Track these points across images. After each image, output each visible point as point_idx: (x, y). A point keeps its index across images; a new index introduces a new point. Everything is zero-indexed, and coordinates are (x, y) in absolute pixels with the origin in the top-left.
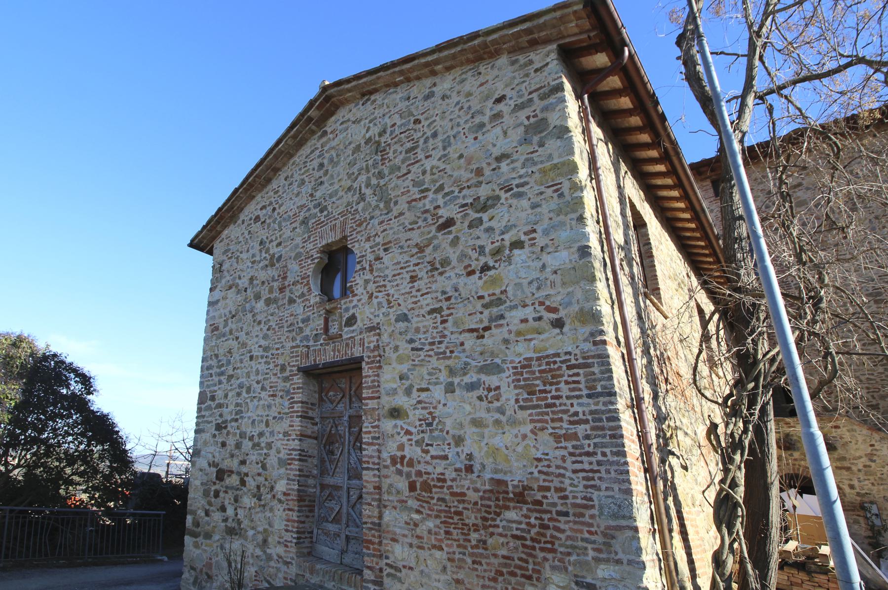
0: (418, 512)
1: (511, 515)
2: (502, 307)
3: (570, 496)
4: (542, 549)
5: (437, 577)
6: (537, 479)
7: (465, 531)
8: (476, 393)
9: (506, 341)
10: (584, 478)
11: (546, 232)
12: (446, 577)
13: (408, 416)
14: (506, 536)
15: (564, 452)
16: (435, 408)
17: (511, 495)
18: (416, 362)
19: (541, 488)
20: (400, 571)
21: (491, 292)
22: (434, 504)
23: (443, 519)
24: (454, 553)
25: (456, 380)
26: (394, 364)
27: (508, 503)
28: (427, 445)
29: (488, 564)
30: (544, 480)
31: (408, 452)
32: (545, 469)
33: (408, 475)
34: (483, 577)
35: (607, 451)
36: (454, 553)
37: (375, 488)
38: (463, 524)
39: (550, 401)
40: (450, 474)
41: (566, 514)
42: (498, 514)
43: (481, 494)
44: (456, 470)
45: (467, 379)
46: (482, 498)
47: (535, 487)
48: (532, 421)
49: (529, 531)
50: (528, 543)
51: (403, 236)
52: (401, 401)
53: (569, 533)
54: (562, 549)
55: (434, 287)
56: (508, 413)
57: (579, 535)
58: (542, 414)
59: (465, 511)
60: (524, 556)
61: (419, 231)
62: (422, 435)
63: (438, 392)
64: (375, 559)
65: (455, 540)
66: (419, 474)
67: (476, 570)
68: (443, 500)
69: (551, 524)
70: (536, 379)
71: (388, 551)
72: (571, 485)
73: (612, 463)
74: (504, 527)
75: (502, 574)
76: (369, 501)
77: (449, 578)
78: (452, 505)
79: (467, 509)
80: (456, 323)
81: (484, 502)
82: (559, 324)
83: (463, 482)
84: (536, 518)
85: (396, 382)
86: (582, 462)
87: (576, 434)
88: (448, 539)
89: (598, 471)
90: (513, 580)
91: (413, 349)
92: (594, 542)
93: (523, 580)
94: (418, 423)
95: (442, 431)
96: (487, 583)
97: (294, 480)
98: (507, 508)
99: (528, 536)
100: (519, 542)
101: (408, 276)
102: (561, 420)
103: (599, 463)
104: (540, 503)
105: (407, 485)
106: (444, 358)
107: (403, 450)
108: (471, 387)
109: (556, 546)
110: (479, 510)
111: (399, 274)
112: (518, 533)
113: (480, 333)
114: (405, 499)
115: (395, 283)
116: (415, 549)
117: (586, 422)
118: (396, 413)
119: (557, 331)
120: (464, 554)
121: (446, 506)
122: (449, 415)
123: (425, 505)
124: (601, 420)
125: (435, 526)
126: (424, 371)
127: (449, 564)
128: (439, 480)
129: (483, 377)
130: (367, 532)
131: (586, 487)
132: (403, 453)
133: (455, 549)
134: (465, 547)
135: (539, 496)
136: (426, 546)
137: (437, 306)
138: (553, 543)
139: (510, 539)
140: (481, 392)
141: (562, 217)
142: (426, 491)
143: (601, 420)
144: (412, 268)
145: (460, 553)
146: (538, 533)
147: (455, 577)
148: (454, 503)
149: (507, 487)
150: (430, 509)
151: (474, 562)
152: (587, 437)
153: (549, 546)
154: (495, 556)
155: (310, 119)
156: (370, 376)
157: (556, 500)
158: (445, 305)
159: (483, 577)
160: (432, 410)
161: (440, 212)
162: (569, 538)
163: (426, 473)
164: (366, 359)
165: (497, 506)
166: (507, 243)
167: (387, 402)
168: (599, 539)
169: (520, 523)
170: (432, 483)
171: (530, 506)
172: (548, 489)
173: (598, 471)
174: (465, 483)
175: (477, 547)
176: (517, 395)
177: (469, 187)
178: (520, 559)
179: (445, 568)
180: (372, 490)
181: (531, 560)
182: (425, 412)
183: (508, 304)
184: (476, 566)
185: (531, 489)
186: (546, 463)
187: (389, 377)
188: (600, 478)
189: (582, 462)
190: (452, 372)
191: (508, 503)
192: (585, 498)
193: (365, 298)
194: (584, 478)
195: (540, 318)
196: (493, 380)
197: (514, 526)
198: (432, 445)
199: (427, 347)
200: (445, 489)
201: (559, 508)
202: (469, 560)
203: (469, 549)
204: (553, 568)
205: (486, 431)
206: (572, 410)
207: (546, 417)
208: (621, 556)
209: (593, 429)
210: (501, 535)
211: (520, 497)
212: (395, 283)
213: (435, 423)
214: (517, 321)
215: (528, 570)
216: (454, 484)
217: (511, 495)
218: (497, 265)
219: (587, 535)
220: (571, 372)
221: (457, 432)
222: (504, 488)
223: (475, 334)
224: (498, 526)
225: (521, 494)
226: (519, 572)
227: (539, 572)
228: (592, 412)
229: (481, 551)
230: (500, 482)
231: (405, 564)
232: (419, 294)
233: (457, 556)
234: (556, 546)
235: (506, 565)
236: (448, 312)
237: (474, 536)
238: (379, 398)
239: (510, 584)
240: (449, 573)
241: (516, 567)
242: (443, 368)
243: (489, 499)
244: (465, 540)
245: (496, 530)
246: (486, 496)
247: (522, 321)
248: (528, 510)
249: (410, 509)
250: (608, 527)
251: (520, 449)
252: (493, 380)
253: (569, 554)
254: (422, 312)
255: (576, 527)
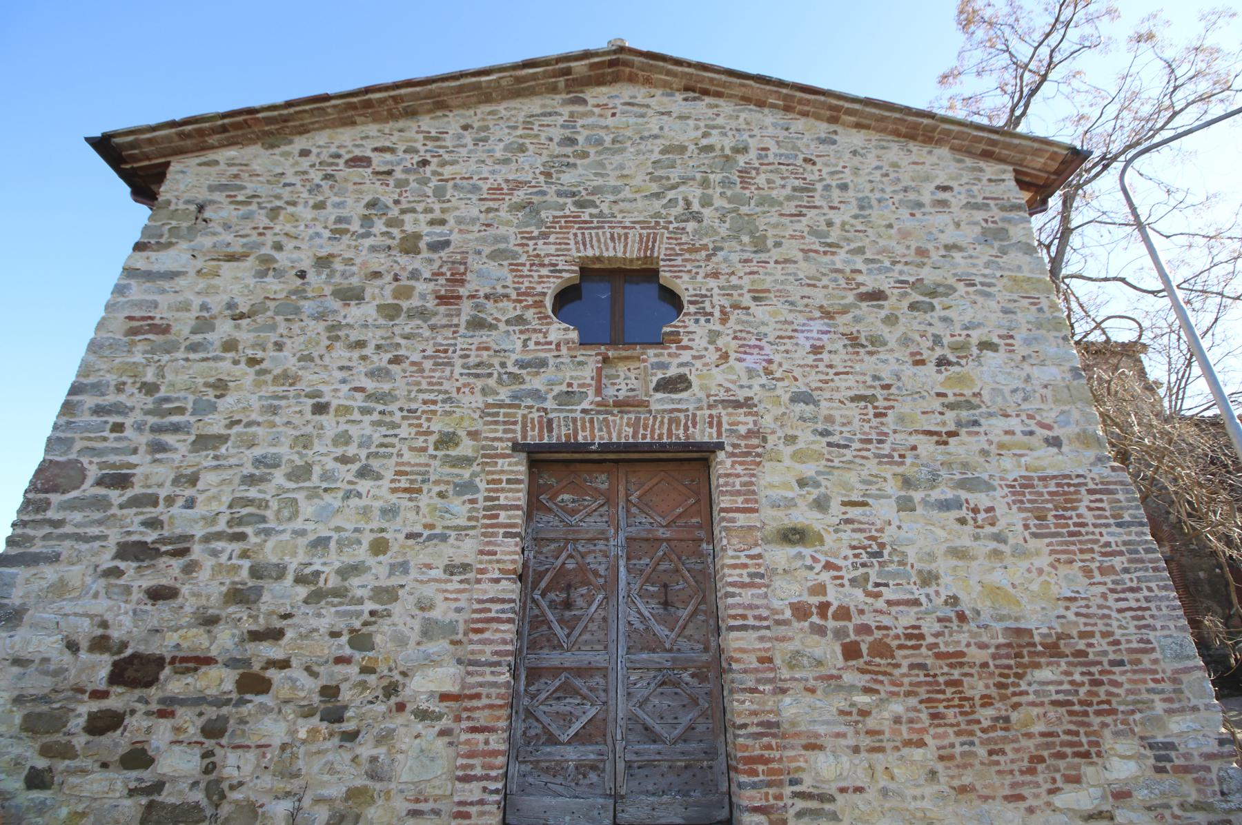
0: (867, 690)
1: (1045, 674)
2: (977, 412)
3: (1123, 640)
4: (1098, 713)
5: (918, 792)
6: (1076, 624)
7: (967, 709)
8: (956, 514)
9: (984, 453)
10: (1134, 618)
11: (1027, 342)
12: (936, 788)
13: (821, 541)
14: (1042, 704)
15: (1102, 589)
16: (881, 530)
17: (1040, 648)
18: (836, 463)
19: (1083, 635)
20: (832, 799)
21: (957, 391)
22: (904, 675)
23: (925, 696)
24: (952, 746)
25: (917, 496)
26: (787, 462)
27: (1037, 659)
28: (877, 585)
29: (1017, 750)
30: (1086, 624)
31: (833, 597)
32: (1084, 611)
33: (839, 633)
34: (1011, 772)
35: (1153, 585)
36: (952, 746)
37: (761, 660)
38: (961, 699)
39: (1072, 528)
40: (929, 626)
41: (1121, 663)
42: (1019, 676)
43: (992, 650)
44: (940, 620)
45: (936, 494)
46: (994, 657)
47: (1074, 633)
48: (1052, 552)
49: (1077, 692)
50: (1077, 708)
51: (796, 292)
52: (803, 516)
53: (1126, 686)
54: (1121, 708)
55: (858, 367)
56: (1011, 541)
57: (1142, 687)
58: (1067, 543)
59: (965, 679)
60: (1073, 727)
61: (825, 291)
62: (862, 570)
63: (884, 510)
64: (771, 791)
65: (952, 725)
66: (864, 629)
67: (997, 763)
68: (922, 666)
69: (1104, 678)
70: (1047, 501)
71: (799, 769)
72: (1120, 627)
73: (1161, 599)
74: (1036, 692)
75: (1041, 760)
76: (751, 684)
77: (945, 788)
78: (938, 672)
79: (971, 675)
80: (901, 419)
81: (998, 662)
82: (1055, 442)
83: (956, 637)
84: (1083, 674)
85: (792, 489)
86: (1126, 599)
87: (1113, 567)
88: (939, 725)
89: (1148, 609)
90: (1062, 764)
91: (829, 444)
92: (1162, 691)
93: (1077, 760)
94: (850, 553)
95: (902, 563)
96: (1019, 778)
97: (498, 664)
98: (1037, 666)
99: (1075, 699)
100: (1063, 710)
101: (808, 344)
102: (1092, 551)
103: (1147, 599)
104: (1082, 653)
105: (838, 649)
106: (891, 463)
107: (825, 594)
108: (945, 505)
109: (1114, 705)
110: (992, 674)
111: (791, 338)
112: (1061, 697)
113: (942, 438)
114: (835, 672)
115: (782, 348)
116: (864, 754)
117: (1121, 553)
118: (794, 536)
119: (1055, 450)
120: (972, 744)
121: (927, 675)
122: (911, 542)
123: (881, 678)
124: (1137, 552)
125: (908, 710)
126: (852, 477)
127: (940, 767)
128: (909, 637)
129: (964, 495)
130: (749, 742)
131: (1139, 628)
132: (823, 599)
133: (952, 738)
134: (972, 733)
135: (1081, 645)
136: (889, 745)
137: (869, 392)
138: (1108, 702)
139: (1048, 707)
140: (963, 513)
141: (1043, 332)
142: (881, 656)
143: (1137, 552)
144: (815, 335)
145: (962, 744)
146: (1090, 693)
147: (956, 783)
148: (941, 669)
149: (1032, 636)
150: (893, 683)
151: (991, 753)
152: (1126, 571)
153: (1106, 707)
154: (1029, 736)
155: (567, 72)
156: (738, 476)
157: (1106, 647)
158: (880, 393)
159: (1011, 772)
160: (874, 533)
161: (860, 278)
162: (1129, 692)
163: (878, 628)
164: (729, 448)
165: (1019, 665)
166: (974, 341)
167: (773, 519)
168: (1167, 686)
169: (1061, 683)
170: (894, 643)
171: (1071, 659)
172: (1091, 634)
173: (1148, 609)
174: (961, 638)
175: (993, 728)
176: (1025, 519)
177: (906, 263)
178: (1069, 732)
179: (933, 773)
180: (755, 664)
181: (1082, 731)
182: (861, 536)
183: (984, 409)
184: (995, 758)
185: (1069, 636)
186: (1083, 603)
187: (775, 479)
188: (1152, 616)
189: (1126, 599)
190: (907, 482)
191: (1037, 659)
192: (1141, 641)
193: (712, 356)
194: (1134, 618)
195: (1031, 433)
196: (982, 500)
197: (1052, 688)
198: (886, 585)
199: (857, 445)
200: (924, 650)
201: (1112, 657)
202: (982, 752)
203: (979, 734)
204: (1117, 734)
205: (974, 564)
206: (1103, 540)
207: (1073, 548)
208: (1194, 702)
209: (1130, 561)
210: (1033, 704)
211: (1053, 649)
212: (782, 348)
213: (886, 552)
214: (999, 431)
215: (1081, 744)
216: (940, 640)
217: (1040, 648)
218: (963, 362)
219: (1152, 685)
220: (1093, 497)
221: (926, 567)
222: (1027, 639)
223: (935, 438)
224: (1027, 693)
225: (1055, 645)
226: (1069, 750)
227: (1097, 744)
228: (1125, 543)
229: (1000, 733)
230: (1019, 632)
231: (843, 784)
232: (832, 371)
233: (958, 750)
234: (1114, 705)
235: (1048, 746)
236: (887, 404)
237: (986, 715)
238: (756, 511)
239: (1058, 770)
240: (942, 780)
241: (1063, 744)
242: (889, 476)
243: (1008, 656)
244: (969, 722)
245: (1023, 699)
246: (1003, 652)
247: (1006, 433)
248: (1069, 664)
249: (851, 688)
250: (1176, 671)
251: (1035, 587)
252: (982, 500)
253: (1133, 712)
254: (837, 396)
255: (1136, 677)
